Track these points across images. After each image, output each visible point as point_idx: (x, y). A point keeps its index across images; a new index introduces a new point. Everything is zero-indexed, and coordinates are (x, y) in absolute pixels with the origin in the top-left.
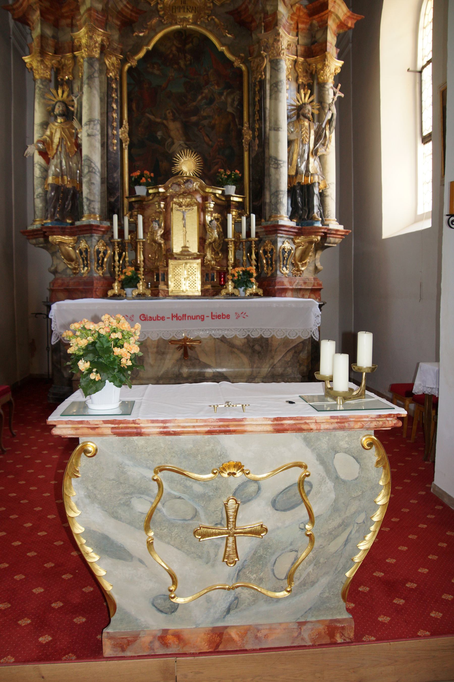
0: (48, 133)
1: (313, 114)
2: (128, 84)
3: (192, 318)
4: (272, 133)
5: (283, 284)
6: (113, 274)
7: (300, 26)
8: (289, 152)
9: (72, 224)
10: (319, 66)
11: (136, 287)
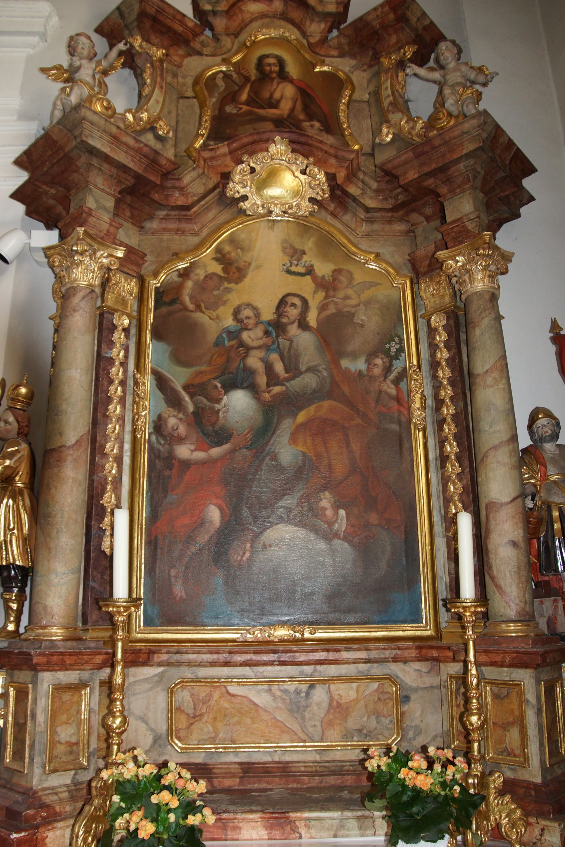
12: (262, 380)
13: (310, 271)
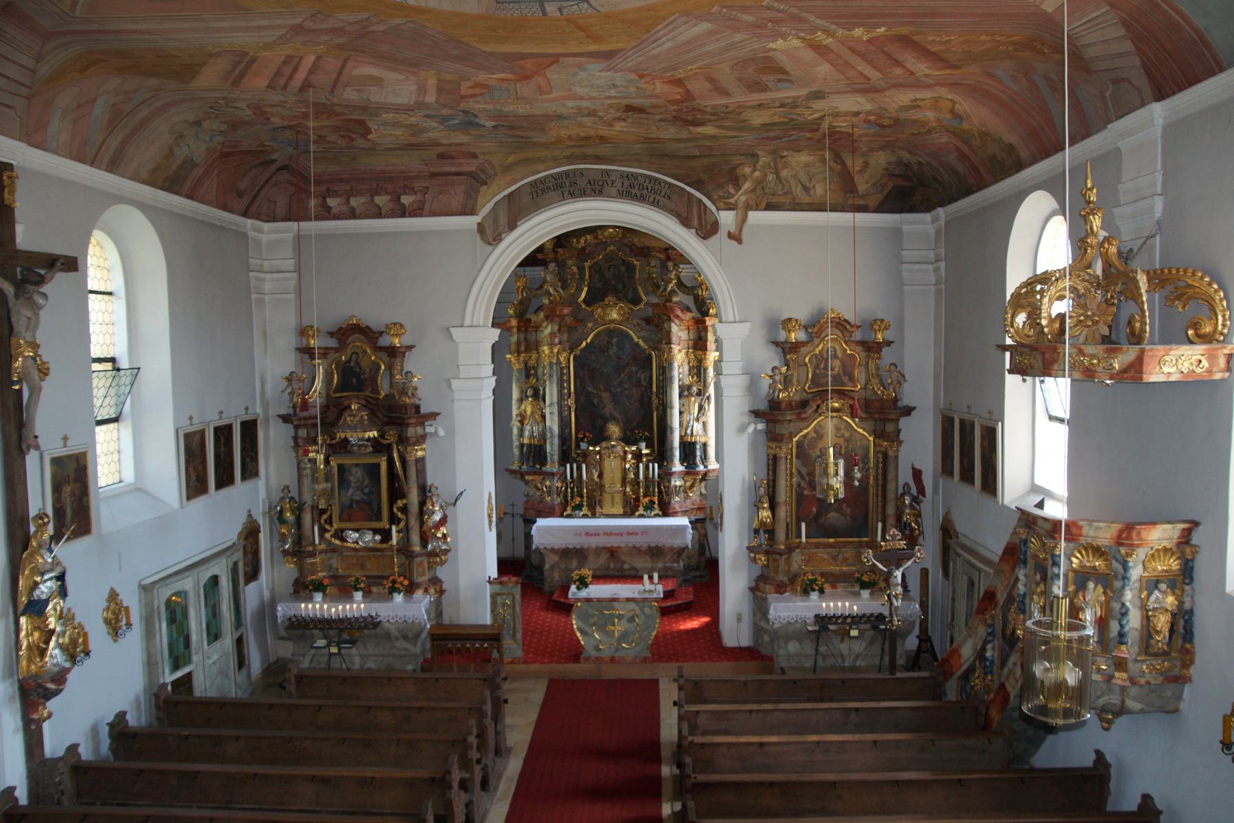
0: (523, 407)
1: (700, 390)
2: (574, 367)
3: (615, 534)
4: (669, 410)
5: (674, 508)
6: (567, 501)
9: (540, 469)
11: (582, 510)
13: (843, 436)
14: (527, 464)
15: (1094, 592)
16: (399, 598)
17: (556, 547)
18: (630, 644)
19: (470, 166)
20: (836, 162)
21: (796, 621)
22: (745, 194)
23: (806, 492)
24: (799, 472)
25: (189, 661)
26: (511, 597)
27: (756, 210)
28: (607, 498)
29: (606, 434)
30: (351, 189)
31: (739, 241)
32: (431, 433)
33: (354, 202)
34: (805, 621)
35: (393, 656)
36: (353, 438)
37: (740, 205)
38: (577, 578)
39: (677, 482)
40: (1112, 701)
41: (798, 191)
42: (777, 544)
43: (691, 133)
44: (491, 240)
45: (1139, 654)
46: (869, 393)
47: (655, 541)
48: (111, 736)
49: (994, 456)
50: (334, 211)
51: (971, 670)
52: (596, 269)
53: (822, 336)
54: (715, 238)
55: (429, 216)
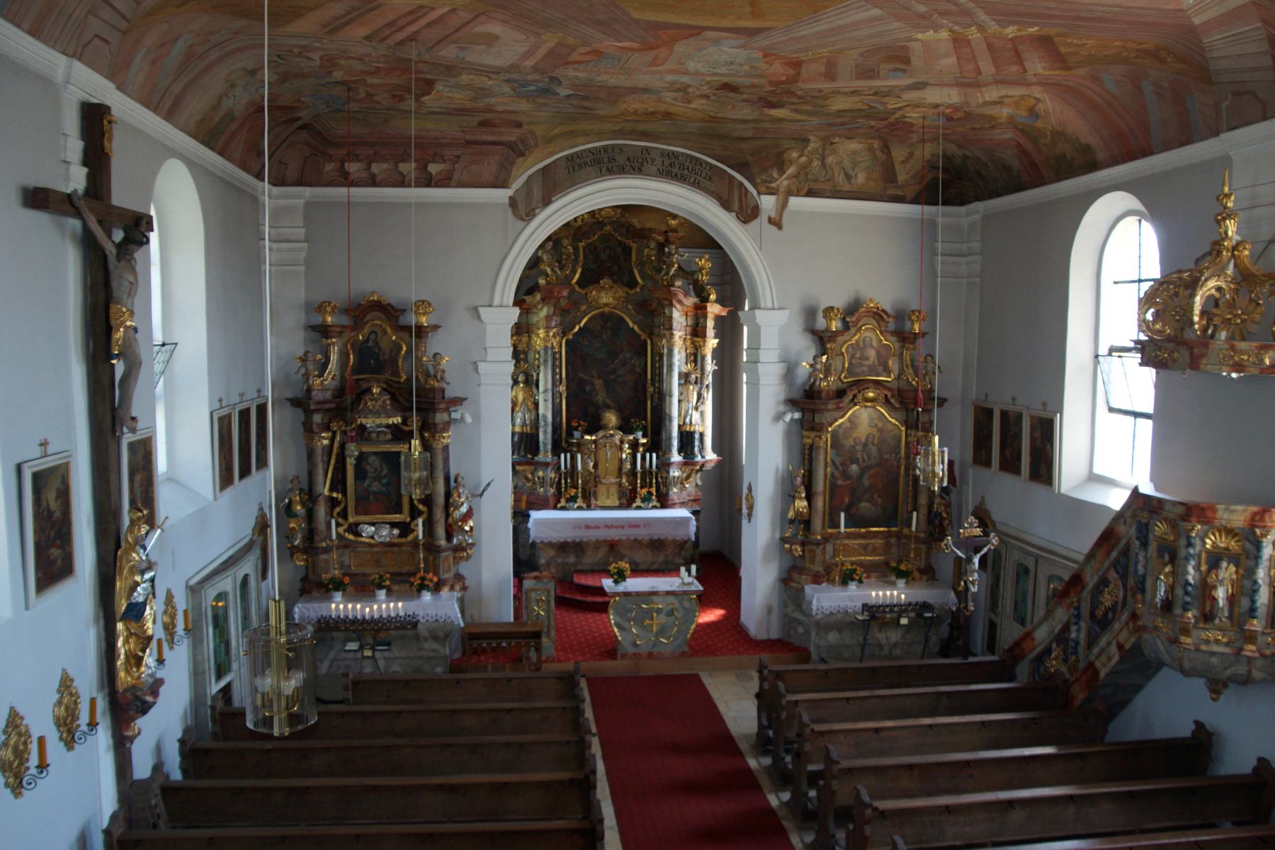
2: (566, 352)
3: (616, 527)
4: (667, 398)
5: (673, 500)
7: (689, 314)
8: (679, 406)
9: (532, 459)
10: (701, 343)
12: (861, 461)
13: (876, 426)
14: (518, 454)
15: (1227, 571)
16: (427, 596)
17: (554, 541)
18: (668, 639)
19: (511, 135)
20: (882, 151)
21: (839, 611)
22: (788, 178)
23: (839, 482)
24: (833, 462)
25: (229, 670)
26: (546, 593)
27: (797, 196)
28: (601, 490)
29: (603, 423)
30: (375, 154)
31: (779, 226)
32: (456, 420)
33: (375, 168)
34: (847, 611)
35: (421, 658)
36: (369, 422)
37: (782, 189)
38: (616, 571)
39: (675, 473)
40: (1240, 672)
41: (840, 179)
42: (814, 534)
43: (761, 114)
44: (524, 217)
45: (1266, 628)
46: (903, 384)
47: (657, 533)
48: (183, 754)
49: (1049, 446)
50: (352, 177)
51: (1047, 651)
52: (591, 249)
53: (859, 326)
54: (755, 223)
55: (457, 187)
